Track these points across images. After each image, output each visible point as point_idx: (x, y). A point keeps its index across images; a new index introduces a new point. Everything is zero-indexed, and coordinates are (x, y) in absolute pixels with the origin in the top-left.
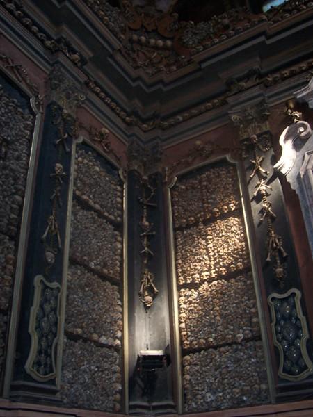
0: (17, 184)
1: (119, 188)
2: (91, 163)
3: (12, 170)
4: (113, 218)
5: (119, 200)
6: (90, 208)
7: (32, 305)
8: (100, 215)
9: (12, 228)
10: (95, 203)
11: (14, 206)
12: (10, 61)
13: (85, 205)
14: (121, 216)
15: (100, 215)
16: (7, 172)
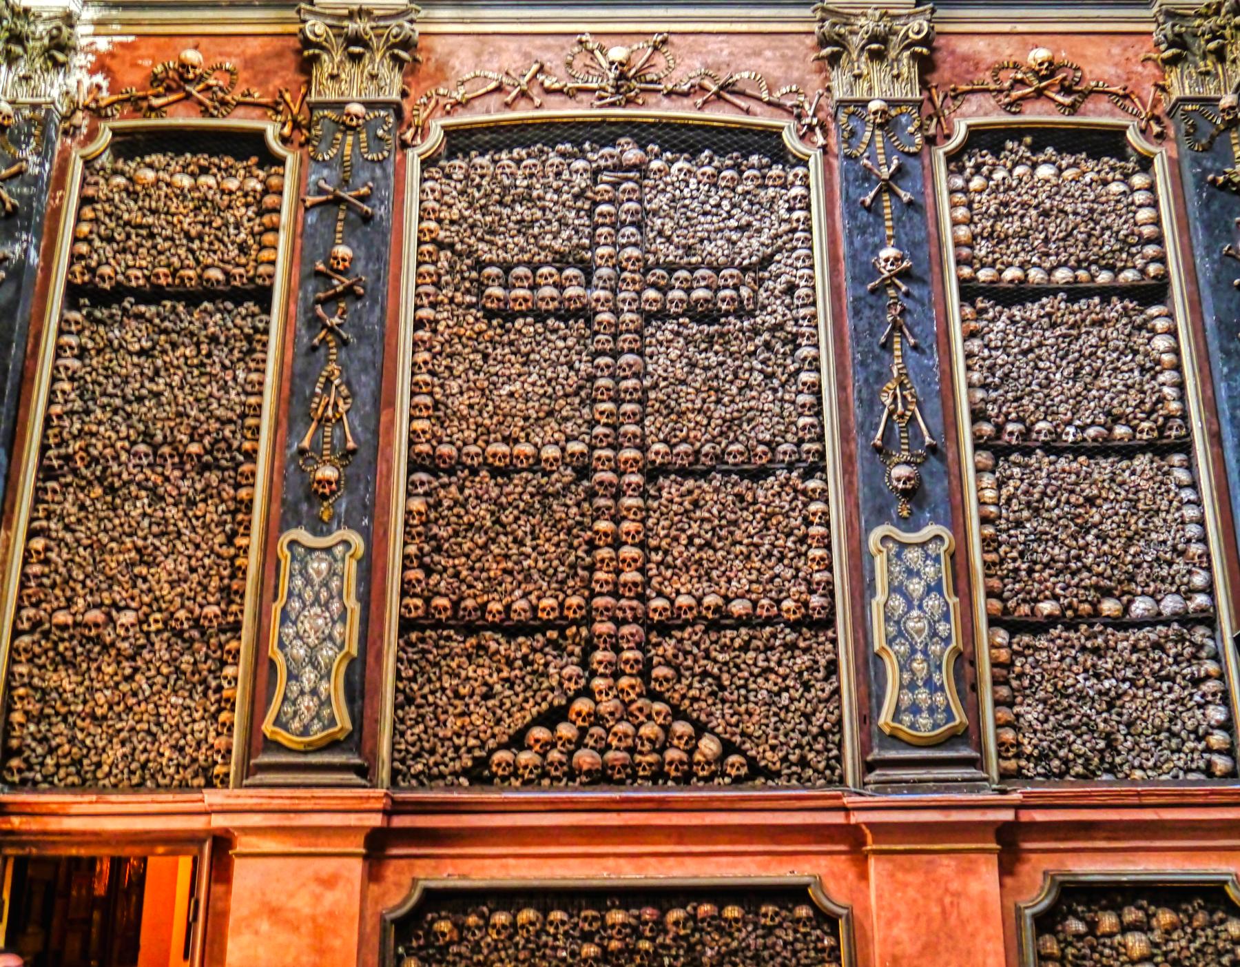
0: (800, 346)
1: (1138, 180)
2: (1019, 170)
3: (779, 326)
4: (1129, 276)
5: (1144, 214)
6: (1036, 294)
7: (873, 595)
8: (1075, 293)
9: (806, 446)
10: (1050, 272)
11: (801, 399)
12: (707, 83)
13: (1020, 294)
14: (1162, 259)
15: (1075, 293)
16: (766, 336)
